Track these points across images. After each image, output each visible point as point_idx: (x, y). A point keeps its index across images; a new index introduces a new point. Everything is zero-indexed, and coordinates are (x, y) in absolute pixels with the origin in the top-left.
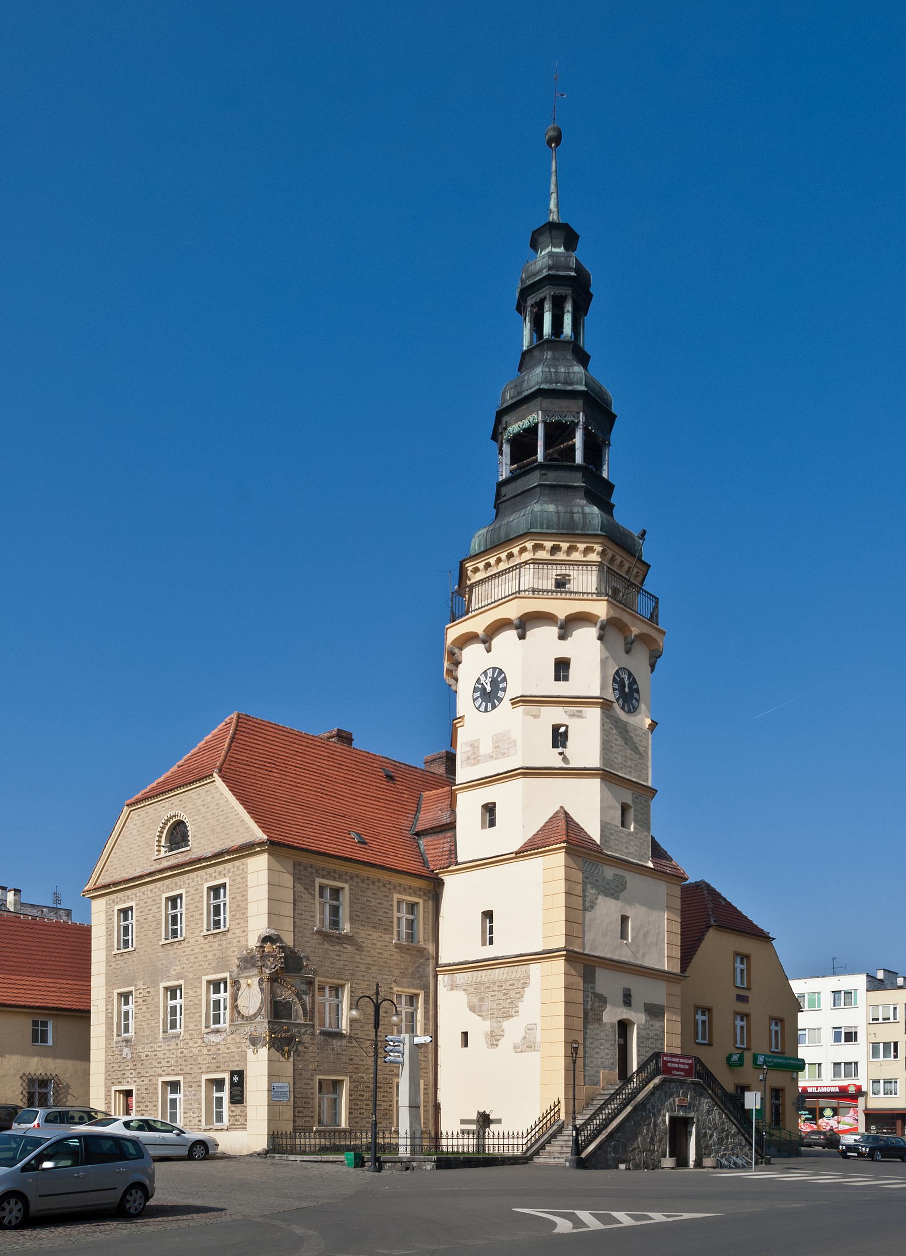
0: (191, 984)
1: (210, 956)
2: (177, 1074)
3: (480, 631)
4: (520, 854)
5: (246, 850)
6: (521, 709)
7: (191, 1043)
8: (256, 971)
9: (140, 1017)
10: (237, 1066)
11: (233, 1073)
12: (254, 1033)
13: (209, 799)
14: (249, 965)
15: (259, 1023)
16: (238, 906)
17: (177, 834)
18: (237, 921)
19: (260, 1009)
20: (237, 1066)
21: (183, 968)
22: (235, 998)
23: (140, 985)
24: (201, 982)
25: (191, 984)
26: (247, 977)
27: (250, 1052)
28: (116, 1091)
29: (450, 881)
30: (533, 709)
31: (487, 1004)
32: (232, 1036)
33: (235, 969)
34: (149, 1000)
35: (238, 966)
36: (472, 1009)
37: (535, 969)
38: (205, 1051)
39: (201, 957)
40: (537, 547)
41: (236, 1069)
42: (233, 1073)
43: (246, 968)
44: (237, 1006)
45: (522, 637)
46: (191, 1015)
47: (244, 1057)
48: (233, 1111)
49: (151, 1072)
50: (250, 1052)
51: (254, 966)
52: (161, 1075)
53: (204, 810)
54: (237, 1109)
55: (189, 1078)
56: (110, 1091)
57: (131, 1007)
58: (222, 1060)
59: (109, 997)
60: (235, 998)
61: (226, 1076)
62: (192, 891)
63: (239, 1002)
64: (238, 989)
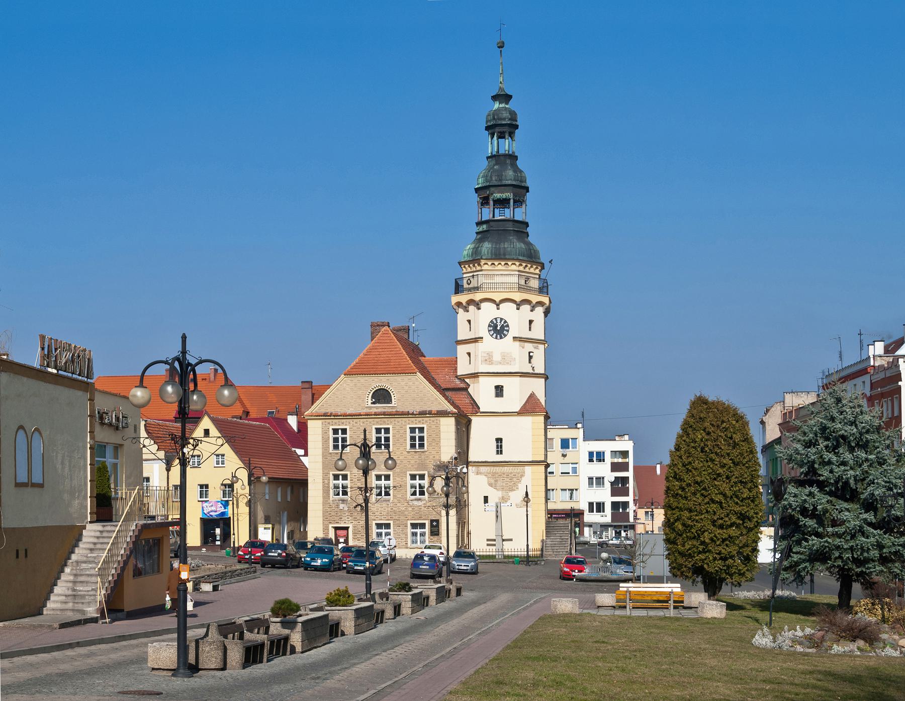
1: (412, 462)
3: (498, 300)
4: (519, 413)
5: (443, 414)
6: (517, 343)
11: (432, 521)
13: (411, 384)
17: (381, 396)
22: (431, 485)
29: (476, 421)
30: (522, 343)
36: (490, 485)
37: (528, 469)
38: (410, 509)
39: (405, 462)
40: (520, 265)
42: (432, 521)
45: (518, 309)
54: (435, 538)
55: (397, 522)
60: (431, 485)
62: (398, 427)
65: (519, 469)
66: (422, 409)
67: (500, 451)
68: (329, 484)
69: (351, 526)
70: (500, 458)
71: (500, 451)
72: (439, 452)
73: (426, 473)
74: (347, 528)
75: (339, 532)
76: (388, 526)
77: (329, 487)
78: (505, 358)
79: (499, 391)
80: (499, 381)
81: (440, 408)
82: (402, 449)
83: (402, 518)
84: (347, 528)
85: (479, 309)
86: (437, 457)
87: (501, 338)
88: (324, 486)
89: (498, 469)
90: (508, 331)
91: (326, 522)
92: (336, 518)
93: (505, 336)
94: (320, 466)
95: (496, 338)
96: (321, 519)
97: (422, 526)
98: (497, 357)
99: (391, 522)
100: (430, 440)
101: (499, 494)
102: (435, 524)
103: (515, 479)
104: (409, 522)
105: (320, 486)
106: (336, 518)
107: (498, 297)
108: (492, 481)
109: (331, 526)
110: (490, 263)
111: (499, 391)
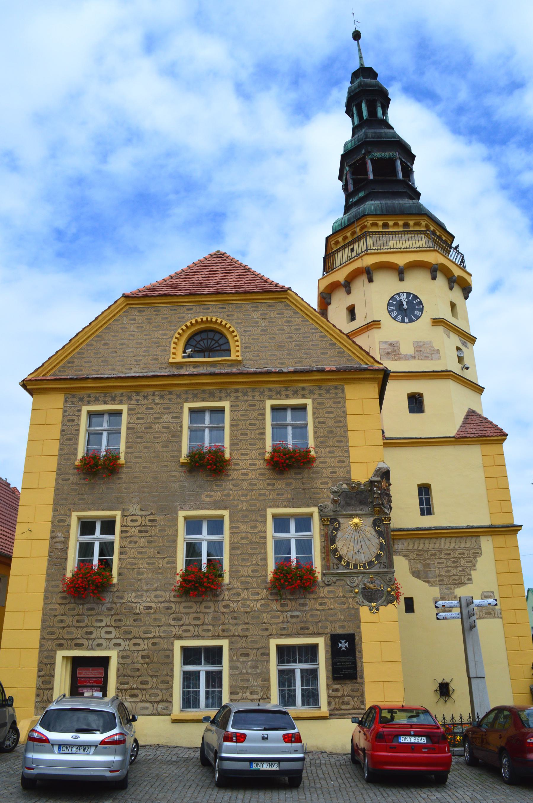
0: (246, 516)
2: (218, 637)
7: (245, 594)
8: (367, 510)
9: (131, 553)
10: (343, 627)
12: (371, 586)
13: (273, 314)
14: (353, 502)
15: (378, 573)
16: (332, 432)
18: (328, 449)
19: (378, 557)
20: (343, 627)
21: (228, 495)
22: (329, 539)
23: (135, 509)
24: (265, 516)
25: (246, 516)
26: (352, 516)
27: (364, 611)
28: (63, 657)
31: (434, 570)
32: (331, 588)
33: (329, 504)
34: (153, 531)
35: (335, 502)
41: (340, 631)
42: (335, 639)
43: (348, 504)
44: (336, 550)
46: (245, 556)
47: (356, 618)
48: (337, 690)
49: (156, 632)
50: (364, 611)
51: (363, 503)
52: (180, 638)
53: (264, 323)
54: (346, 688)
55: (242, 643)
56: (54, 658)
57: (116, 538)
58: (311, 619)
59: (59, 524)
61: (321, 642)
63: (339, 545)
64: (337, 529)
65: (469, 544)
66: (300, 367)
67: (427, 509)
68: (65, 542)
69: (113, 655)
70: (427, 522)
71: (427, 509)
72: (345, 461)
73: (315, 510)
74: (104, 662)
75: (84, 673)
76: (214, 655)
77: (65, 550)
78: (422, 350)
79: (416, 403)
80: (415, 387)
81: (343, 364)
82: (253, 454)
83: (254, 630)
84: (104, 662)
85: (371, 280)
86: (341, 473)
87: (411, 321)
88: (52, 548)
89: (429, 545)
90: (422, 310)
91: (49, 645)
92: (77, 633)
93: (418, 318)
94: (49, 497)
95: (403, 321)
96: (35, 638)
97: (310, 652)
98: (406, 349)
99: (225, 644)
100: (322, 432)
101: (436, 591)
102: (343, 645)
103: (463, 562)
104: (273, 643)
105: (43, 548)
106: (77, 633)
107: (401, 260)
108: (419, 566)
109: (60, 654)
110: (380, 223)
111: (416, 403)
